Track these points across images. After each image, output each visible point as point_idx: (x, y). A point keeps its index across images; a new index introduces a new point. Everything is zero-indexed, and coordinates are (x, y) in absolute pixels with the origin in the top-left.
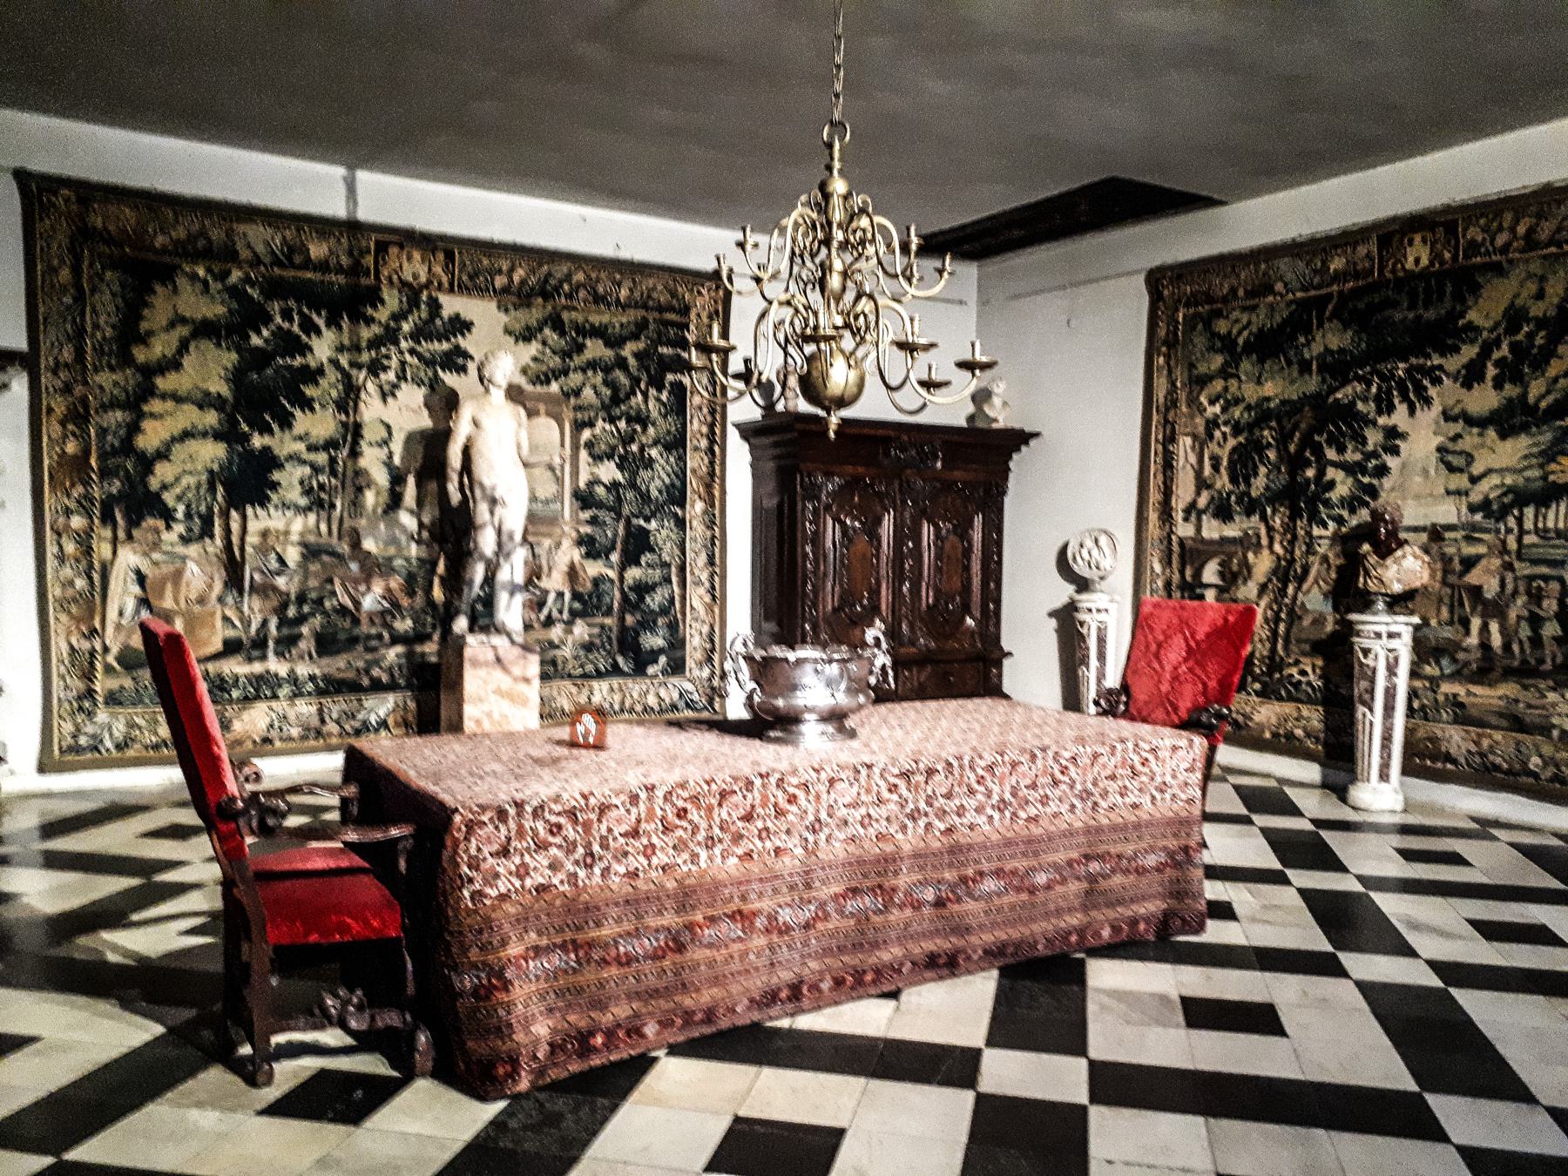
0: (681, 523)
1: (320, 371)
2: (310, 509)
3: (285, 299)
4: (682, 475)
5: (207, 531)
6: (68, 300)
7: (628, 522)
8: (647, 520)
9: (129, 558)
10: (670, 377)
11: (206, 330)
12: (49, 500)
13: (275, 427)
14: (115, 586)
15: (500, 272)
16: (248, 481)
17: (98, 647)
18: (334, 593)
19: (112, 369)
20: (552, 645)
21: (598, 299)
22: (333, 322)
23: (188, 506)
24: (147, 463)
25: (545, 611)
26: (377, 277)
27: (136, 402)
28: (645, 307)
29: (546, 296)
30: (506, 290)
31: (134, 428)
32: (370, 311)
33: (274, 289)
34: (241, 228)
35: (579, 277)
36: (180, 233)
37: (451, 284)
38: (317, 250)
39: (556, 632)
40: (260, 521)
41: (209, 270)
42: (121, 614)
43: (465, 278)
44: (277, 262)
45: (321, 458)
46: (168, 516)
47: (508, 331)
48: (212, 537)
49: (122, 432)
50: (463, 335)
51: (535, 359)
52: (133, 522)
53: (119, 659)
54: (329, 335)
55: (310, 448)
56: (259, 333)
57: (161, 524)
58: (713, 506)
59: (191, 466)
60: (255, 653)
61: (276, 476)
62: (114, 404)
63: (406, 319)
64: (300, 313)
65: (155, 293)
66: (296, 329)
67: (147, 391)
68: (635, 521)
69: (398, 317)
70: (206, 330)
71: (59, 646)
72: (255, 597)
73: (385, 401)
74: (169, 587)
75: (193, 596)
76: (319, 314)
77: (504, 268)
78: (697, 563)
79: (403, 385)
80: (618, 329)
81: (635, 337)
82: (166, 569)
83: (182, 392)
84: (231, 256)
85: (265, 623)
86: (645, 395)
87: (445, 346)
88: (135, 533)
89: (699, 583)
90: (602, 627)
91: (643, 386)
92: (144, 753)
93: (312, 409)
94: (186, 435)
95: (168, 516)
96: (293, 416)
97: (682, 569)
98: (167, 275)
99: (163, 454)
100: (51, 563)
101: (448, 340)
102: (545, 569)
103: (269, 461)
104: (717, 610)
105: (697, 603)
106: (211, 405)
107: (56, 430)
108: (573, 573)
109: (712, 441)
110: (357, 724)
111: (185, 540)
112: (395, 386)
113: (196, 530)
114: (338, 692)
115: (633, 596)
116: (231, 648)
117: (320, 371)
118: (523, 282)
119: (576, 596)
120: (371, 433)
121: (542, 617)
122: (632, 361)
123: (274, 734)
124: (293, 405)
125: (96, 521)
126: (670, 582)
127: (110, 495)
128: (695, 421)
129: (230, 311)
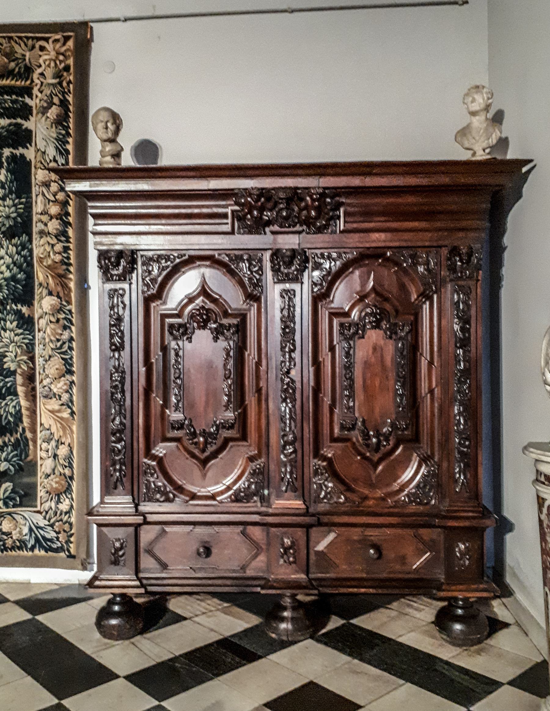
0: (27, 323)
4: (26, 266)
10: (7, 152)
78: (48, 369)
97: (30, 378)
126: (16, 394)
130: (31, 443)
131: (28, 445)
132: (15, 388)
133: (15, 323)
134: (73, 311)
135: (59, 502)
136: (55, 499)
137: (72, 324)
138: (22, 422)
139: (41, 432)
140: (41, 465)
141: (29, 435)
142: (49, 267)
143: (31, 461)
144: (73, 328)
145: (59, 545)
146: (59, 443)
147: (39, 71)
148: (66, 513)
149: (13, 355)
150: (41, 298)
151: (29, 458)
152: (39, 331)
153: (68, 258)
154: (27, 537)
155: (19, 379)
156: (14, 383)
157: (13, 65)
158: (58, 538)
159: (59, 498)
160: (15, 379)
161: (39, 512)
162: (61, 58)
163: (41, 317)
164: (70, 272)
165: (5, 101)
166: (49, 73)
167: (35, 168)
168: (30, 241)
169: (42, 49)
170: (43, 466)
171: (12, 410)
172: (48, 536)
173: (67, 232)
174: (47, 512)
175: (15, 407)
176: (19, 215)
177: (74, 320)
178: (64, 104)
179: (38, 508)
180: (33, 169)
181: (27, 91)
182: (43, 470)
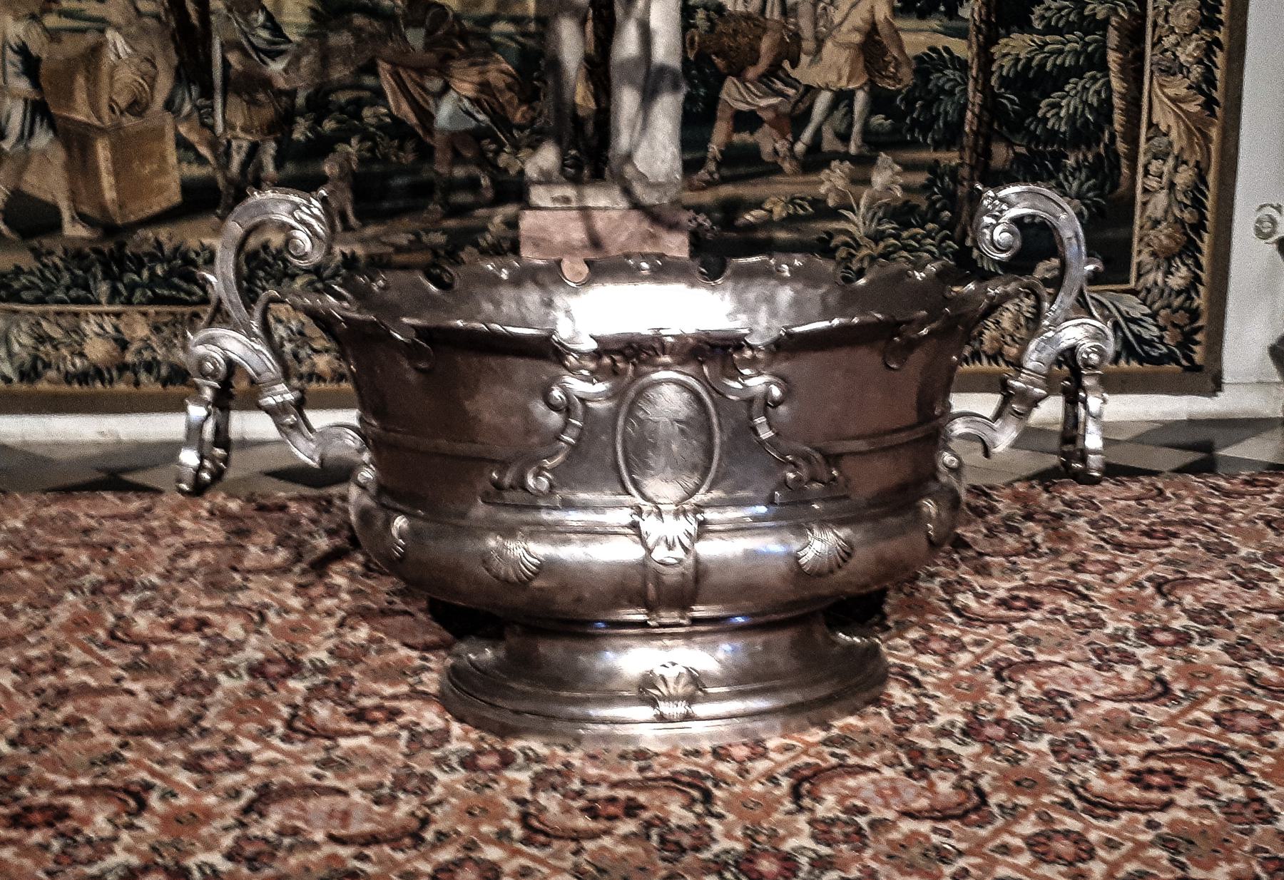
18: (379, 94)
20: (822, 210)
25: (807, 135)
39: (832, 181)
72: (233, 100)
74: (80, 81)
75: (123, 101)
82: (72, 46)
85: (254, 149)
89: (1173, 69)
90: (933, 168)
92: (65, 388)
97: (1134, 36)
102: (808, 45)
104: (1214, 133)
105: (1164, 117)
108: (872, 48)
115: (1010, 101)
119: (879, 101)
121: (799, 147)
126: (1104, 68)
130: (1124, 162)
131: (1119, 168)
132: (1104, 55)
135: (1168, 273)
136: (1164, 266)
138: (1110, 122)
139: (1148, 140)
140: (1145, 204)
141: (1121, 147)
143: (1122, 197)
145: (1165, 350)
146: (1179, 161)
148: (1179, 293)
151: (1121, 189)
155: (1113, 38)
156: (1102, 47)
158: (1161, 338)
159: (1170, 266)
160: (1104, 36)
170: (1150, 206)
171: (1093, 100)
172: (1146, 335)
174: (1149, 291)
175: (1098, 93)
179: (1132, 284)
182: (1148, 213)
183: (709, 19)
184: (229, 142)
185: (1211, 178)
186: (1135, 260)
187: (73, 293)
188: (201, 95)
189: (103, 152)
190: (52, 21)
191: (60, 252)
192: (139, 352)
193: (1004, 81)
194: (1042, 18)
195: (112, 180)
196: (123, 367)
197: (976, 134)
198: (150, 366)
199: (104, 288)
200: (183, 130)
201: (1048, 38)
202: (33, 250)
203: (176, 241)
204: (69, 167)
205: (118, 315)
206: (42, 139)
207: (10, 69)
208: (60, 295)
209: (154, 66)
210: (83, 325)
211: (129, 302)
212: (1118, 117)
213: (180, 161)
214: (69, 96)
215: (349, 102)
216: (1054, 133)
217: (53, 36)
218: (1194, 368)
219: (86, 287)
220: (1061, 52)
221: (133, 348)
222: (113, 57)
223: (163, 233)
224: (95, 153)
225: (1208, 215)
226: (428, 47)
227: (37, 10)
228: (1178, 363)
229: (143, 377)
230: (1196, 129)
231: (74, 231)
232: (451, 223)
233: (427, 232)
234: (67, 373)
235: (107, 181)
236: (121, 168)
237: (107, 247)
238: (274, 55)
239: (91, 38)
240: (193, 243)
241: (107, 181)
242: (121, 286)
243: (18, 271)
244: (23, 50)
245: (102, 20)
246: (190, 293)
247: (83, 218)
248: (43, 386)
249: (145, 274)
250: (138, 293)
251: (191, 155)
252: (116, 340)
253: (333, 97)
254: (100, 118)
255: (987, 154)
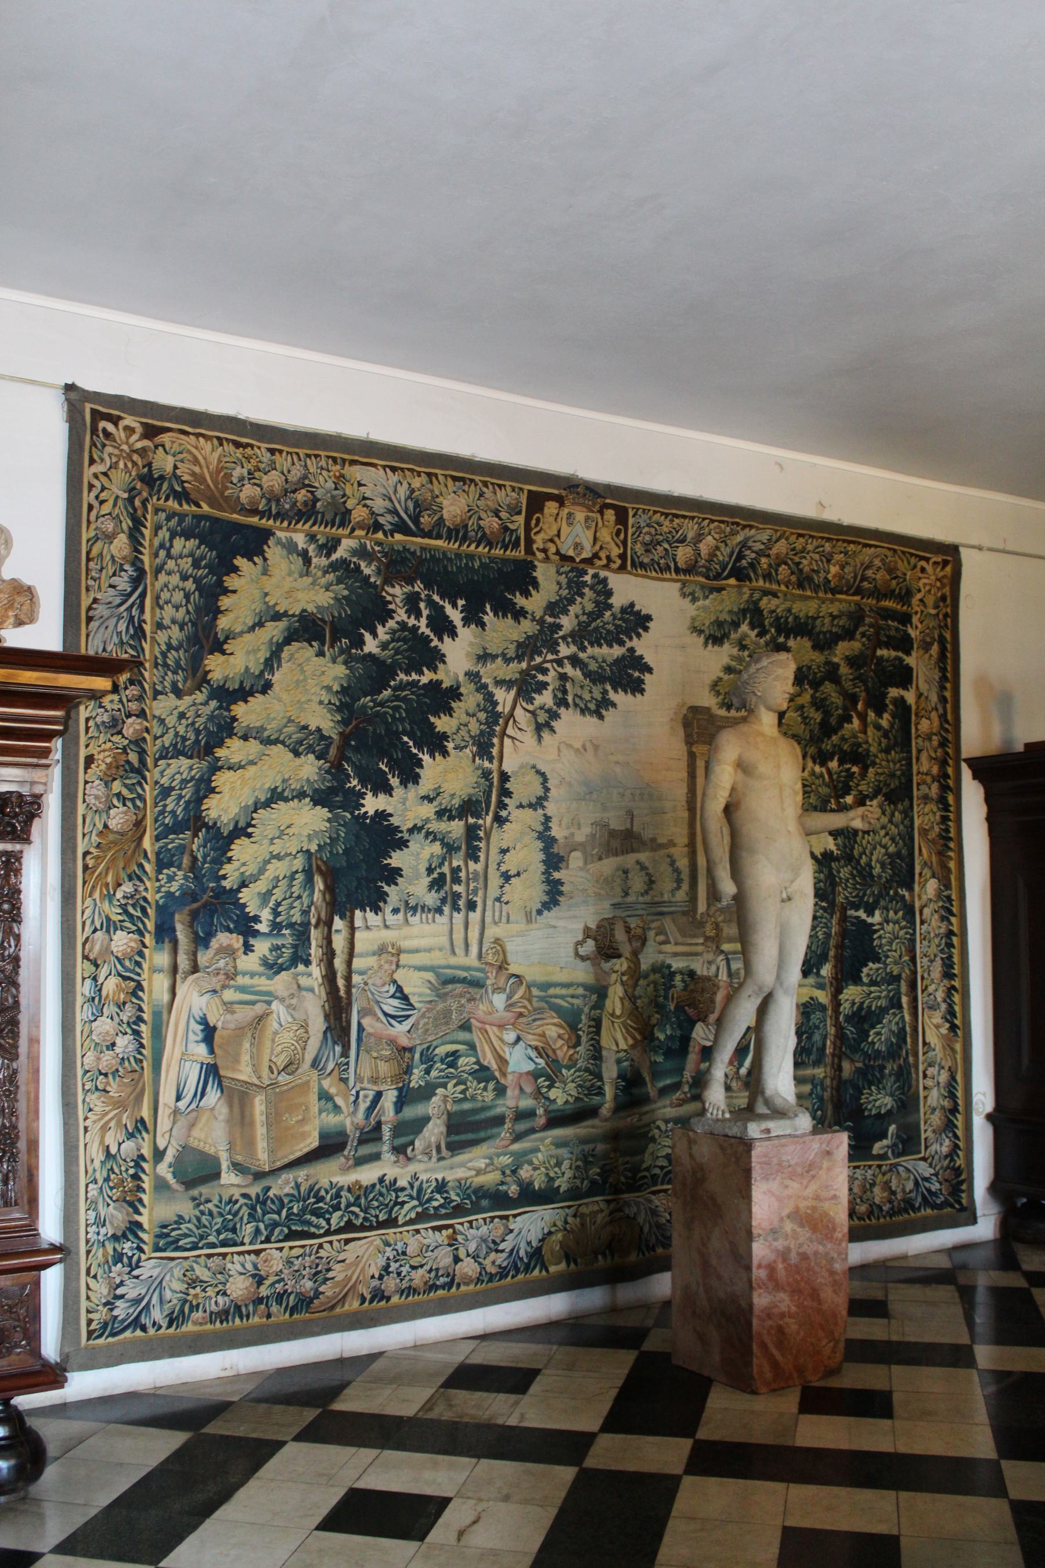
1: (455, 693)
2: (439, 911)
3: (410, 582)
4: (908, 838)
5: (300, 957)
6: (123, 583)
7: (844, 918)
8: (870, 913)
9: (193, 999)
11: (307, 629)
12: (86, 908)
13: (394, 782)
14: (172, 1051)
15: (682, 540)
16: (357, 871)
17: (146, 1151)
19: (179, 693)
21: (804, 581)
22: (473, 617)
23: (276, 913)
24: (223, 841)
26: (529, 550)
27: (208, 743)
28: (859, 591)
29: (740, 574)
30: (690, 570)
31: (205, 788)
32: (520, 601)
33: (397, 565)
34: (356, 473)
35: (781, 548)
36: (273, 481)
37: (623, 557)
38: (453, 506)
40: (372, 930)
41: (312, 538)
42: (178, 1098)
43: (639, 548)
44: (401, 527)
45: (456, 828)
46: (246, 927)
47: (697, 630)
48: (307, 963)
49: (188, 793)
50: (639, 636)
51: (728, 670)
52: (201, 941)
53: (177, 1168)
54: (466, 634)
55: (440, 814)
56: (375, 635)
57: (236, 941)
58: (948, 887)
59: (279, 844)
60: (365, 1150)
61: (396, 859)
62: (176, 751)
63: (566, 612)
64: (430, 603)
65: (236, 569)
66: (424, 628)
67: (224, 729)
68: (851, 913)
69: (556, 608)
70: (307, 629)
71: (92, 1152)
73: (540, 738)
74: (247, 1045)
75: (281, 1061)
76: (454, 605)
77: (690, 535)
79: (562, 711)
80: (827, 620)
81: (849, 634)
83: (271, 730)
84: (343, 517)
86: (863, 717)
87: (617, 651)
88: (203, 958)
89: (933, 1007)
91: (860, 706)
93: (445, 753)
94: (275, 797)
95: (246, 927)
96: (419, 763)
97: (913, 986)
98: (254, 543)
99: (241, 831)
100: (82, 1013)
101: (622, 643)
103: (384, 835)
105: (932, 1038)
106: (310, 749)
107: (97, 789)
109: (945, 788)
110: (501, 1259)
111: (273, 968)
112: (554, 715)
113: (287, 953)
114: (477, 1209)
115: (850, 1030)
116: (330, 1146)
117: (455, 693)
118: (712, 555)
120: (523, 788)
121: (743, 1071)
122: (844, 670)
123: (391, 1284)
124: (420, 749)
125: (148, 940)
126: (900, 1007)
127: (169, 895)
128: (924, 756)
129: (336, 599)
132: (899, 999)
133: (901, 913)
134: (953, 897)
137: (953, 915)
138: (905, 1042)
140: (925, 1097)
142: (933, 841)
144: (953, 920)
147: (919, 596)
148: (946, 1157)
149: (896, 955)
150: (926, 881)
152: (922, 922)
153: (947, 831)
154: (913, 1195)
157: (894, 582)
161: (924, 1159)
162: (938, 584)
163: (925, 906)
164: (950, 849)
165: (889, 627)
166: (930, 600)
167: (916, 715)
168: (911, 807)
169: (923, 570)
171: (894, 1028)
173: (945, 798)
175: (897, 1023)
176: (903, 774)
177: (954, 910)
178: (942, 641)
180: (913, 717)
181: (905, 619)
183: (683, 981)
184: (358, 1093)
185: (959, 1077)
186: (923, 1136)
187: (222, 1237)
188: (342, 1056)
189: (259, 1106)
190: (229, 995)
191: (216, 1201)
192: (272, 1285)
193: (848, 1019)
194: (868, 975)
195: (264, 1131)
196: (259, 1301)
197: (833, 1055)
198: (280, 1297)
199: (249, 1228)
200: (326, 1083)
201: (872, 989)
202: (194, 1199)
203: (311, 1182)
204: (229, 1121)
205: (257, 1253)
206: (213, 1095)
207: (192, 1037)
208: (212, 1239)
209: (307, 1032)
210: (229, 1266)
211: (268, 1240)
212: (909, 1040)
213: (320, 1112)
214: (237, 1060)
215: (447, 1055)
216: (879, 1052)
217: (229, 1007)
218: (963, 1209)
219: (234, 1230)
220: (879, 997)
221: (267, 1283)
222: (276, 1025)
223: (301, 1174)
224: (252, 1106)
225: (960, 1102)
226: (509, 1007)
227: (218, 988)
228: (952, 1207)
229: (274, 1308)
230: (948, 1045)
231: (229, 1178)
232: (516, 1147)
233: (498, 1156)
234: (211, 1313)
235: (261, 1131)
236: (273, 1119)
237: (254, 1191)
238: (401, 1019)
239: (260, 1008)
240: (324, 1183)
241: (261, 1131)
242: (262, 1226)
243: (180, 1220)
244: (204, 1021)
245: (268, 993)
246: (318, 1227)
247: (237, 1167)
248: (189, 1327)
249: (284, 1213)
250: (277, 1231)
251: (330, 1105)
252: (254, 1276)
253: (437, 1051)
254: (259, 1078)
255: (840, 1069)
